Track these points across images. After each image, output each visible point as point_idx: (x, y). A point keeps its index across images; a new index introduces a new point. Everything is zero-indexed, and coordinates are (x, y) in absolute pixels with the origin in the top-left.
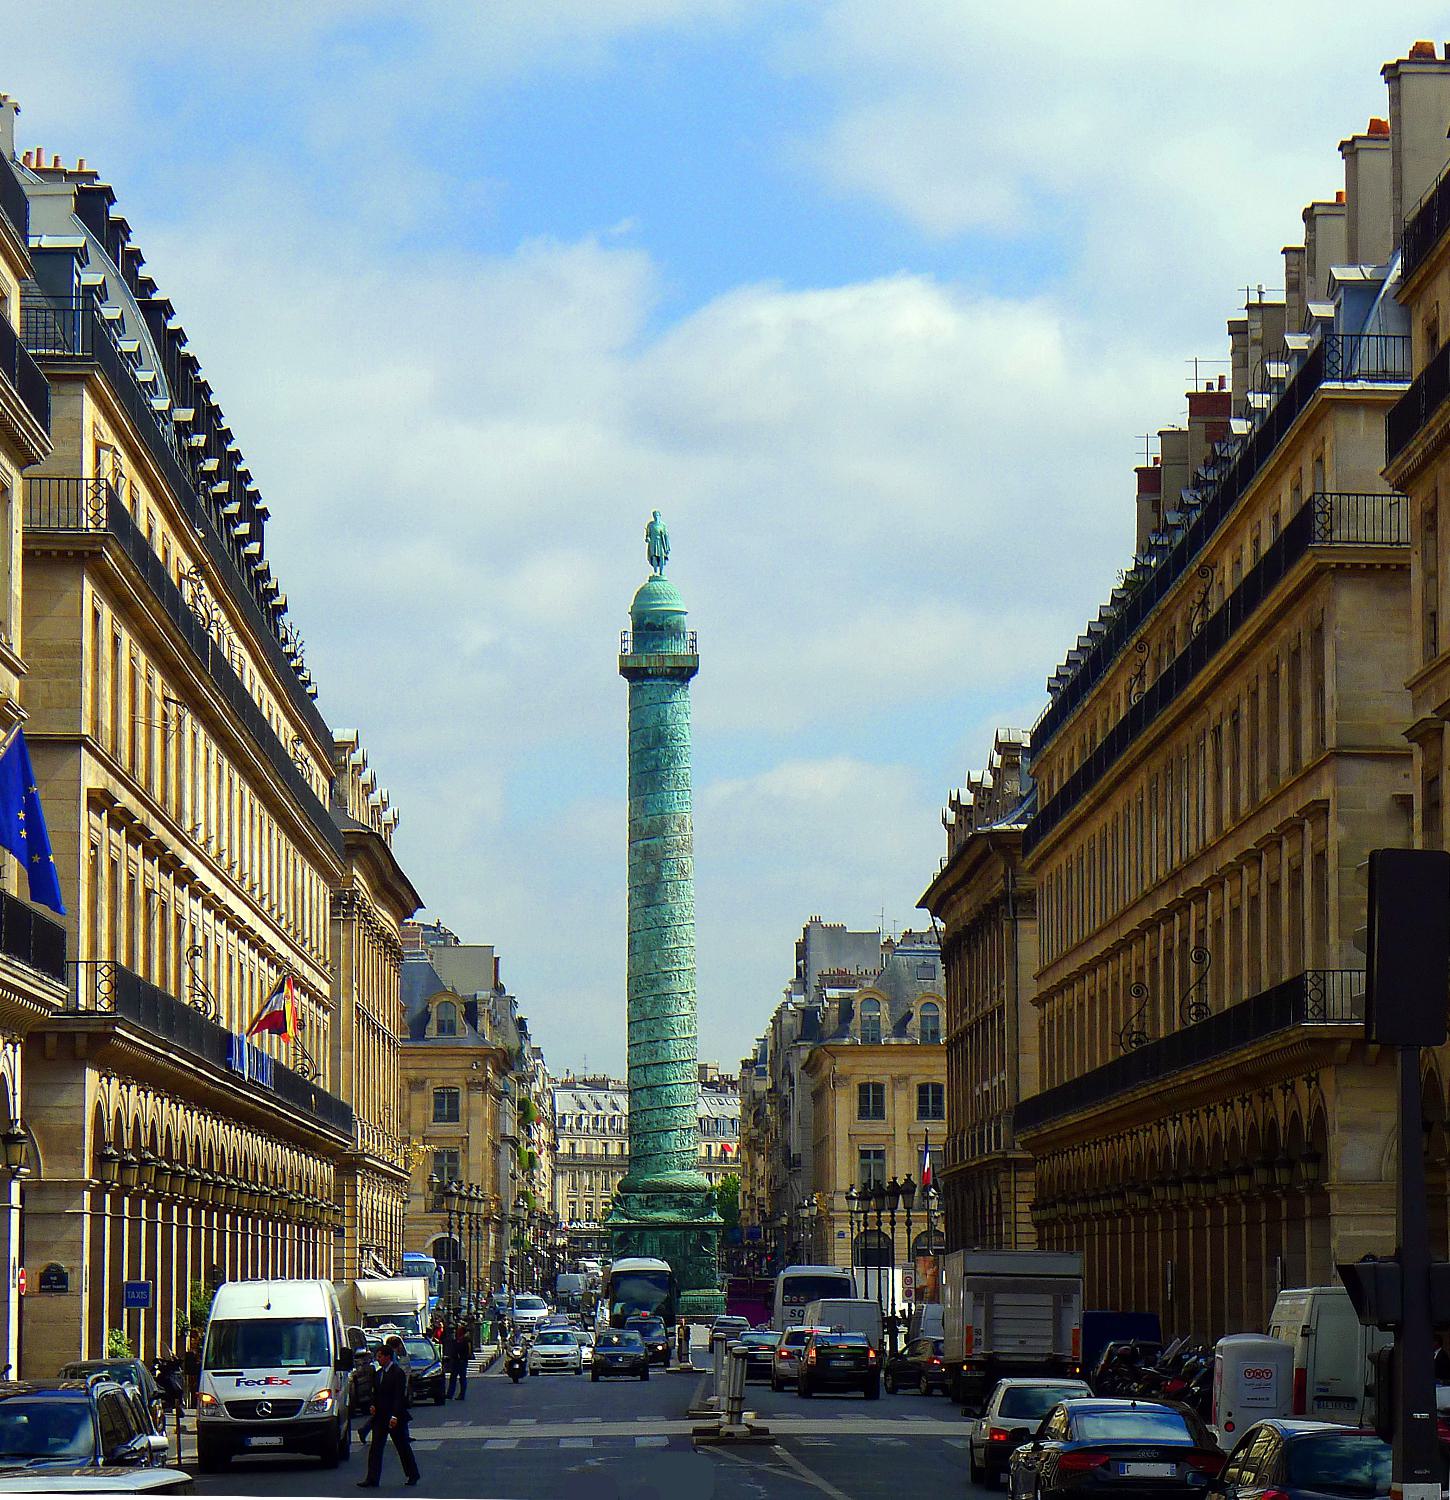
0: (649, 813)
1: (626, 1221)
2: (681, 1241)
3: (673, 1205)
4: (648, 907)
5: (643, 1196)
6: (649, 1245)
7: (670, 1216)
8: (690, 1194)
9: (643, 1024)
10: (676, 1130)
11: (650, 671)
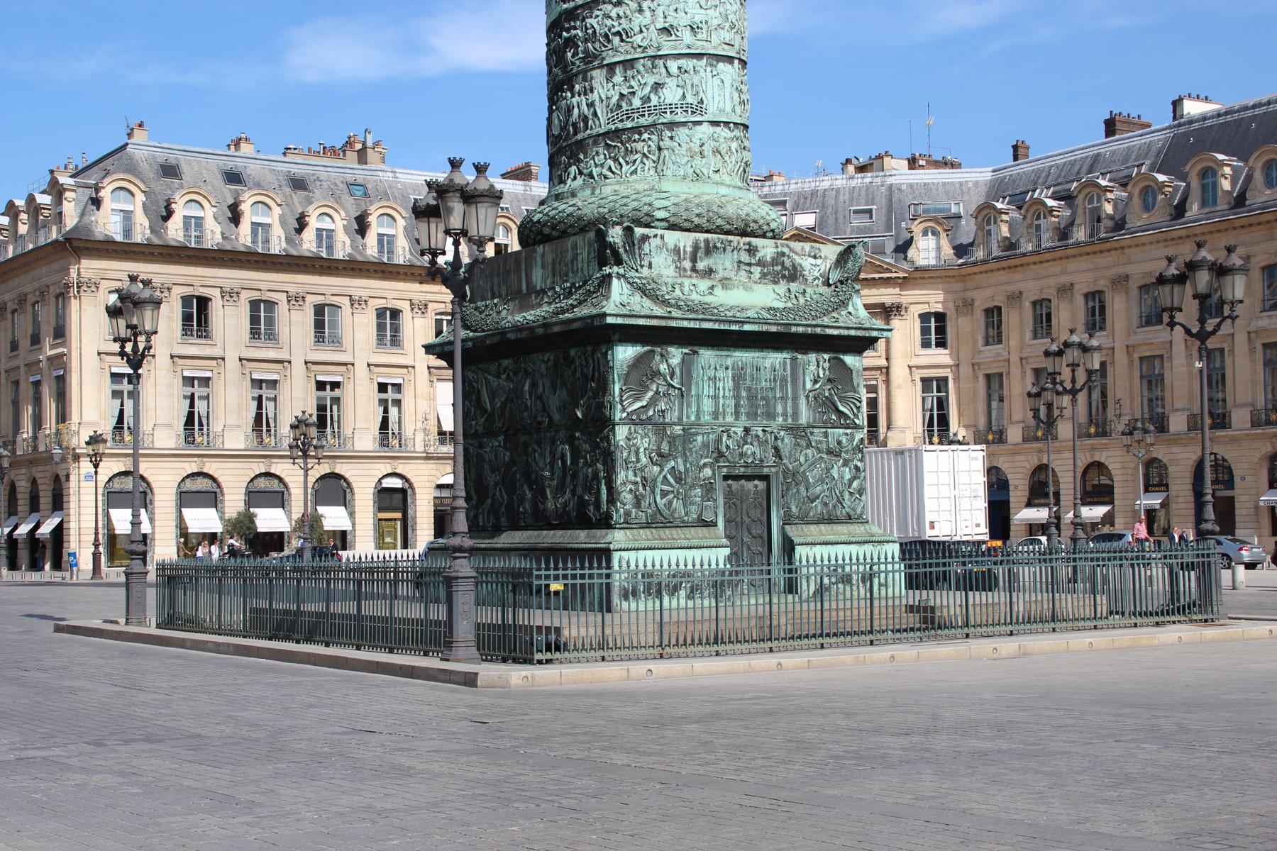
2: (784, 380)
3: (757, 270)
5: (684, 240)
8: (797, 246)
10: (730, 59)
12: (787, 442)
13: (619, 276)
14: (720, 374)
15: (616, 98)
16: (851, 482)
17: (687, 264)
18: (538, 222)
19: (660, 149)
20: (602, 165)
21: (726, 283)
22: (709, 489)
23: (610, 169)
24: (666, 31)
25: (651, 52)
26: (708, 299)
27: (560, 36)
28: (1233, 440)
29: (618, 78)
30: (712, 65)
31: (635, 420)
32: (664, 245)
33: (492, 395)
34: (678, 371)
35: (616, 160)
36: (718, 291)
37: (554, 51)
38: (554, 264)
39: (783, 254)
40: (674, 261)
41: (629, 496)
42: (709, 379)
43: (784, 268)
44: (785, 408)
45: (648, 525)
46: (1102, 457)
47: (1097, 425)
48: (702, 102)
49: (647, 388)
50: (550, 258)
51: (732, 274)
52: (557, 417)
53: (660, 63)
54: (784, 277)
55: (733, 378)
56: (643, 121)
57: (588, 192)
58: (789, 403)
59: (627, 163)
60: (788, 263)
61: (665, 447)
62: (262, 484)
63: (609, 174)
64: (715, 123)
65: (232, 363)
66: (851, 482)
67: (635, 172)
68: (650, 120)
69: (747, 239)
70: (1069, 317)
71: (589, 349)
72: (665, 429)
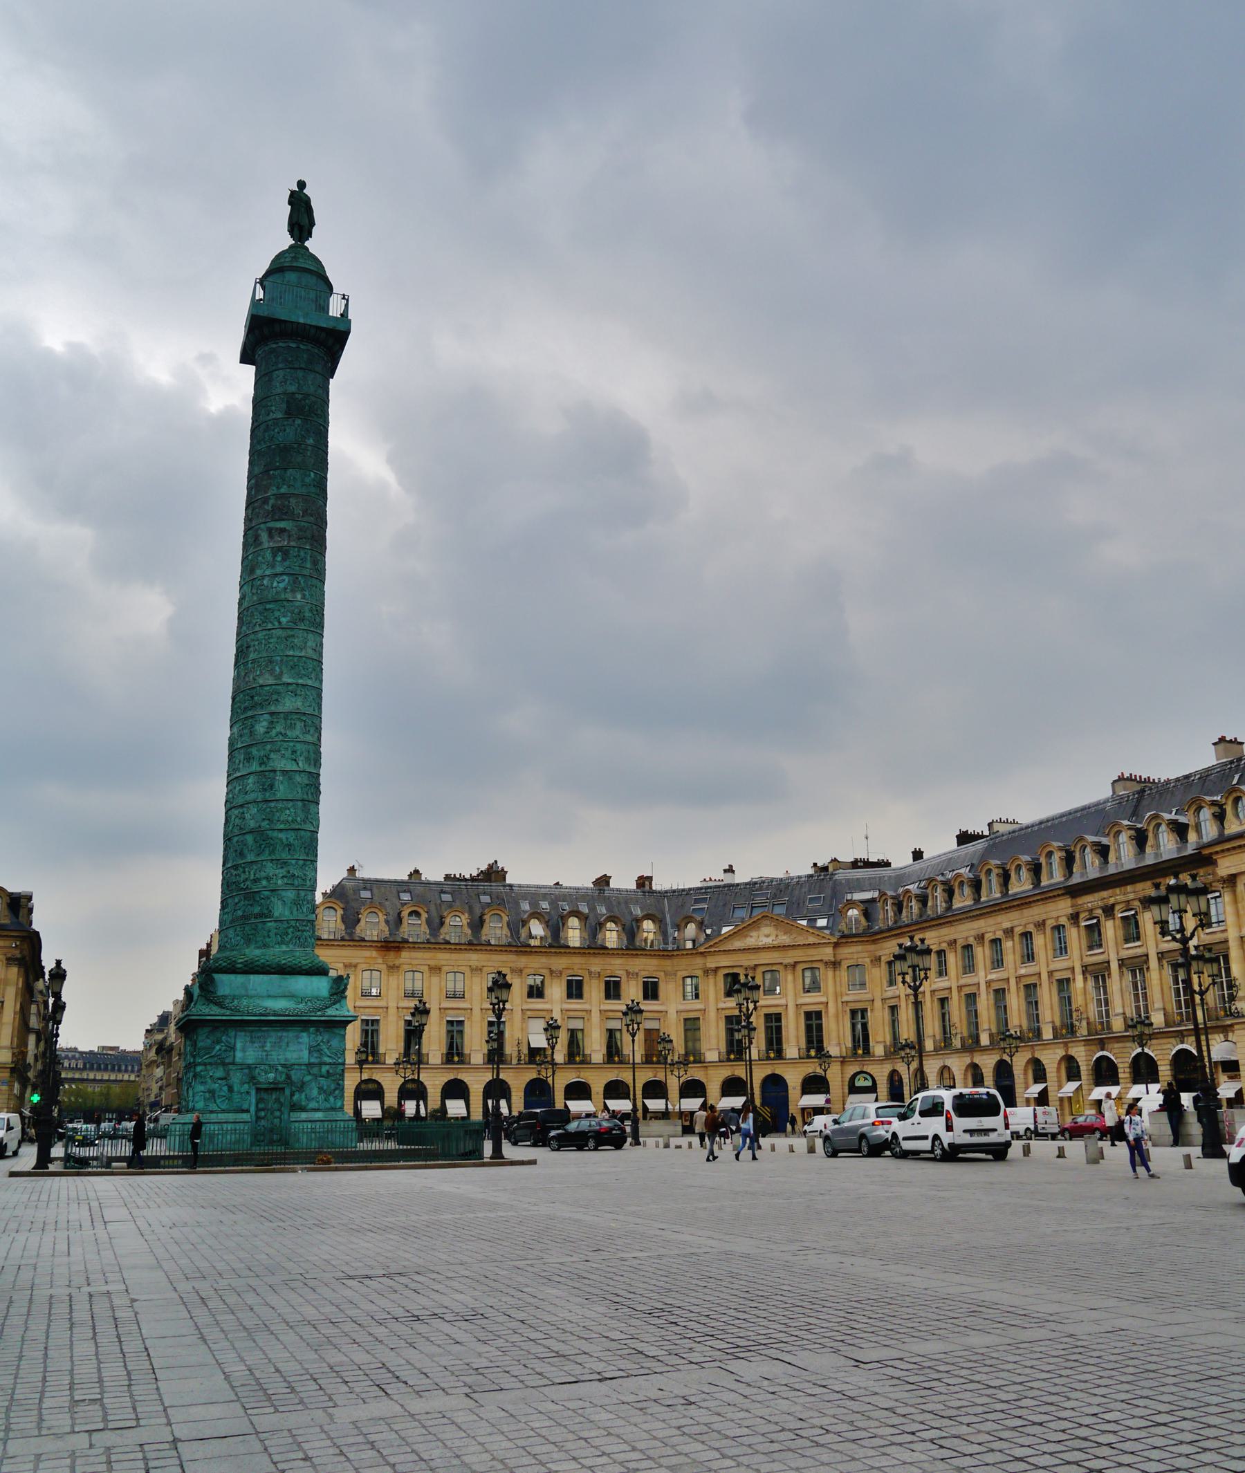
9: (254, 751)
62: (409, 1086)
65: (392, 1011)
70: (632, 992)
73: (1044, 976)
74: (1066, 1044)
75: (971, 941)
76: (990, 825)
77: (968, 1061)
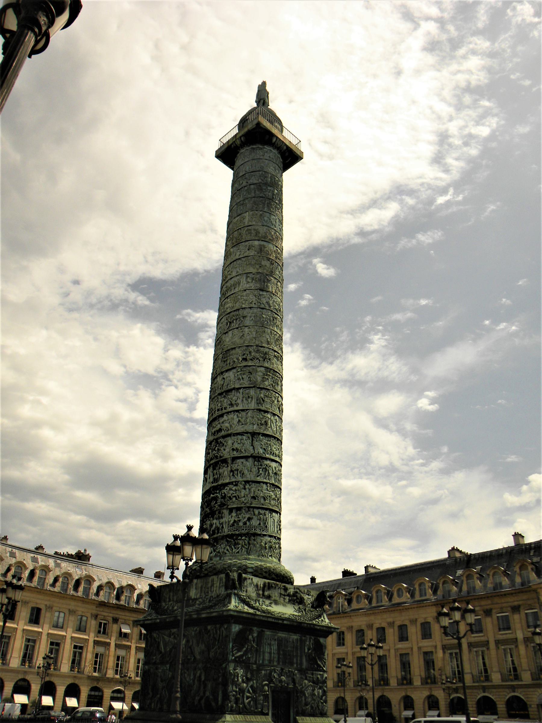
0: (265, 224)
1: (251, 611)
4: (262, 290)
5: (260, 581)
6: (267, 649)
7: (287, 610)
9: (252, 392)
11: (274, 140)
12: (298, 676)
13: (235, 594)
14: (273, 642)
15: (232, 522)
16: (322, 696)
17: (261, 592)
18: (195, 569)
19: (249, 544)
20: (224, 548)
21: (276, 603)
22: (266, 697)
23: (228, 550)
24: (254, 498)
25: (248, 505)
26: (269, 608)
27: (210, 496)
28: (391, 690)
29: (234, 514)
30: (271, 513)
31: (238, 661)
32: (253, 583)
33: (165, 645)
34: (256, 639)
35: (230, 547)
36: (273, 605)
37: (206, 501)
38: (202, 587)
39: (297, 592)
40: (256, 590)
41: (233, 698)
42: (268, 644)
43: (297, 598)
44: (297, 660)
45: (239, 713)
46: (364, 694)
47: (341, 683)
48: (266, 527)
49: (244, 647)
50: (200, 585)
51: (278, 599)
52: (198, 657)
53: (252, 509)
54: (297, 602)
55: (277, 645)
56: (243, 531)
57: (218, 559)
58: (299, 659)
59: (235, 548)
60: (298, 595)
61: (249, 676)
63: (227, 552)
64: (271, 536)
66: (322, 696)
67: (238, 552)
68: (246, 531)
69: (284, 584)
71: (218, 626)
72: (249, 666)
73: (415, 649)
74: (430, 689)
75: (363, 627)
76: (366, 568)
77: (358, 695)
